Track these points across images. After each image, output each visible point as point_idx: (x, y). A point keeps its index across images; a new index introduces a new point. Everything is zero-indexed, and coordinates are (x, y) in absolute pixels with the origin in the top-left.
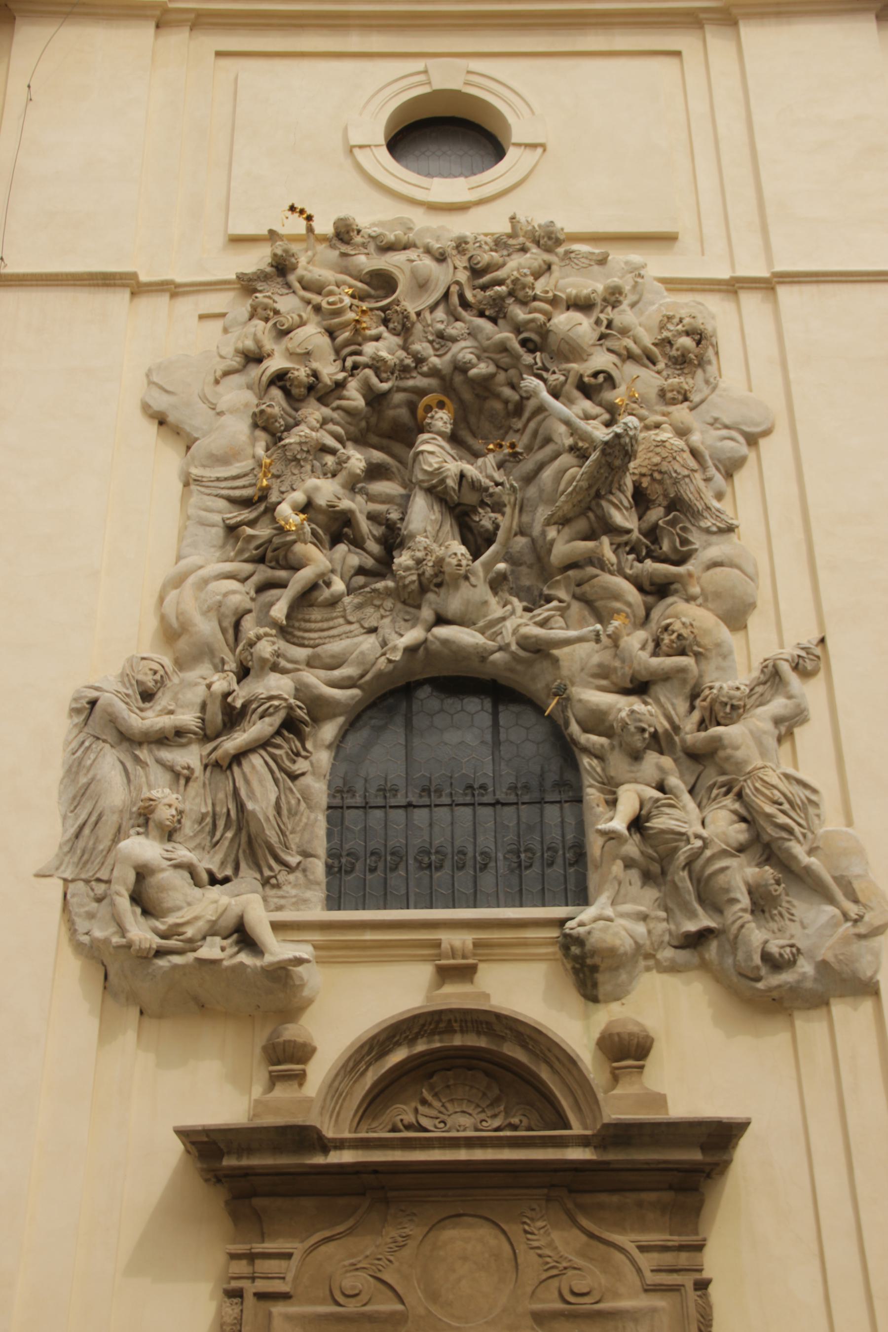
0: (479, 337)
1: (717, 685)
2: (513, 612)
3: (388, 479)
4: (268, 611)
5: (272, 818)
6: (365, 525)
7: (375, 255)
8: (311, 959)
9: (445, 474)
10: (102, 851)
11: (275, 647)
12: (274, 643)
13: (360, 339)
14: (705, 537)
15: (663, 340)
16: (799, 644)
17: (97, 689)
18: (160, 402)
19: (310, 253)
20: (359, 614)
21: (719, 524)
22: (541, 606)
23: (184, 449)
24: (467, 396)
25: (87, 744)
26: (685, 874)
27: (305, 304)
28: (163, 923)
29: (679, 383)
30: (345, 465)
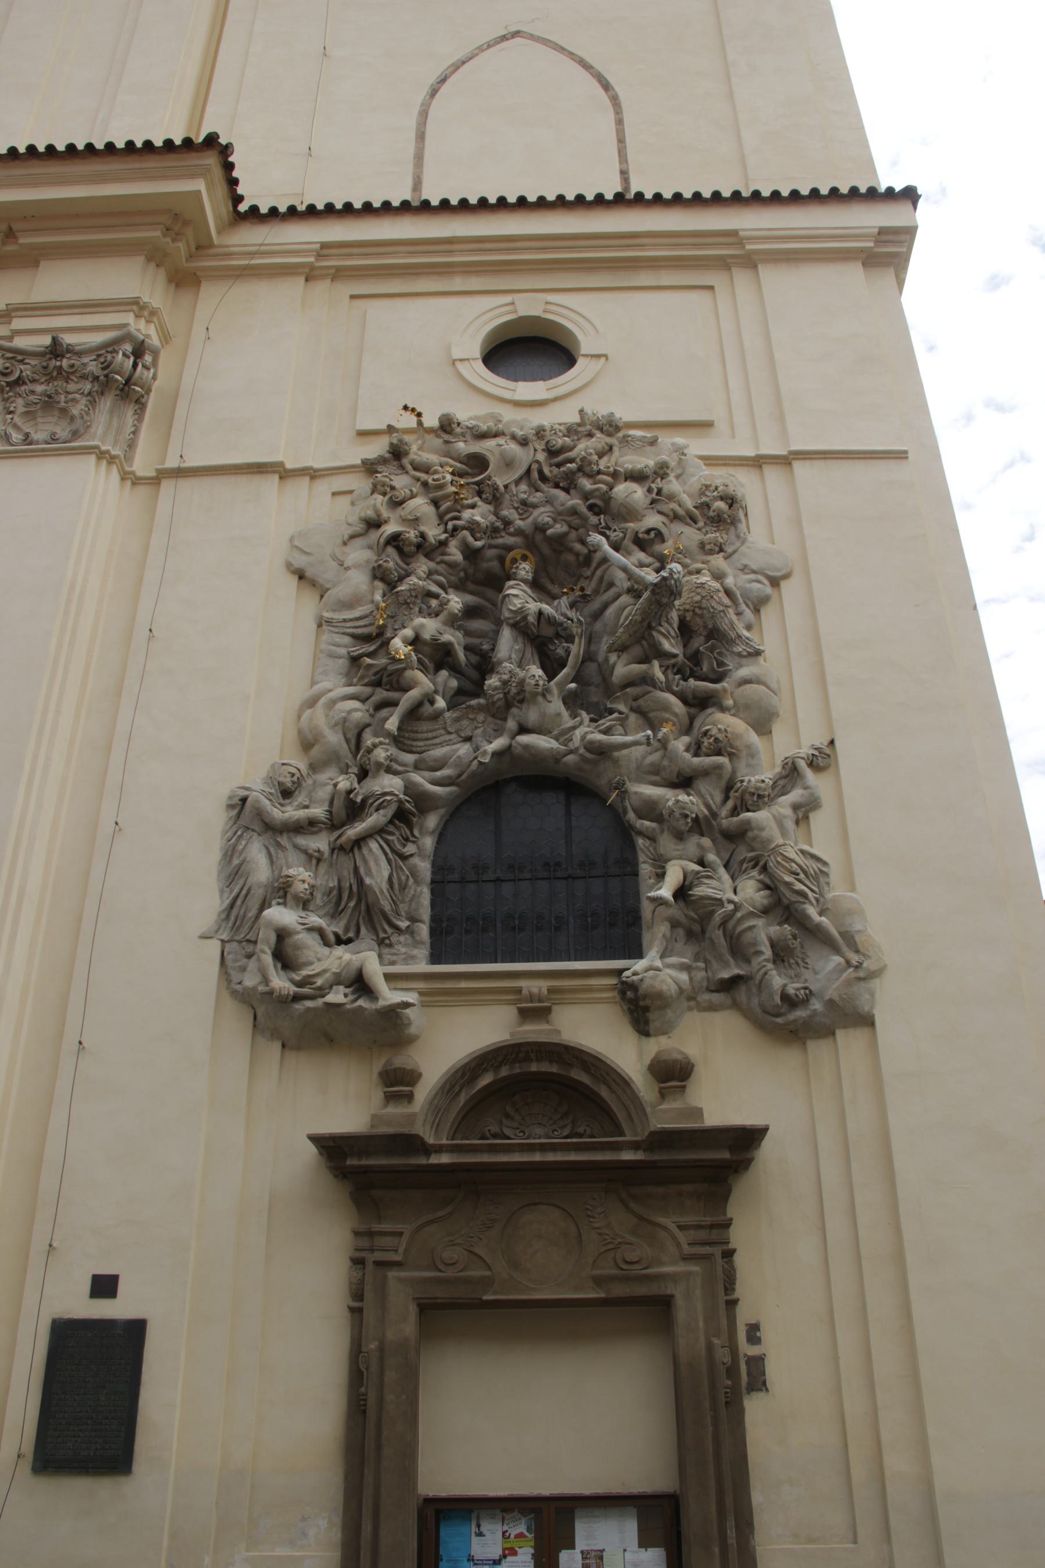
0: (555, 504)
1: (746, 779)
2: (581, 723)
3: (483, 618)
4: (384, 725)
5: (385, 890)
6: (461, 655)
7: (471, 442)
8: (416, 1003)
9: (527, 613)
10: (251, 918)
11: (389, 754)
12: (387, 750)
13: (459, 507)
14: (737, 659)
15: (702, 504)
16: (813, 745)
17: (247, 789)
18: (300, 561)
19: (420, 442)
20: (457, 726)
21: (748, 649)
22: (606, 717)
23: (319, 597)
24: (546, 550)
25: (239, 833)
26: (721, 932)
27: (416, 481)
28: (298, 975)
29: (715, 537)
30: (445, 607)
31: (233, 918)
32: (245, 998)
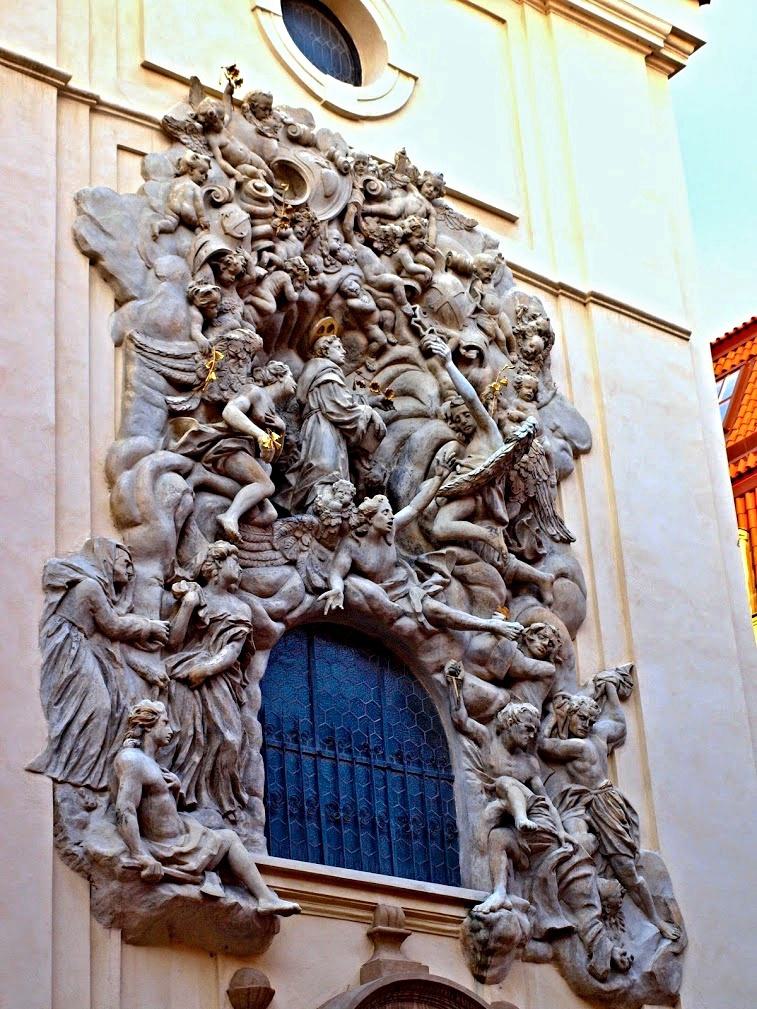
0: (367, 268)
10: (93, 756)
15: (520, 331)
18: (95, 243)
30: (281, 379)
31: (67, 749)
32: (90, 867)
